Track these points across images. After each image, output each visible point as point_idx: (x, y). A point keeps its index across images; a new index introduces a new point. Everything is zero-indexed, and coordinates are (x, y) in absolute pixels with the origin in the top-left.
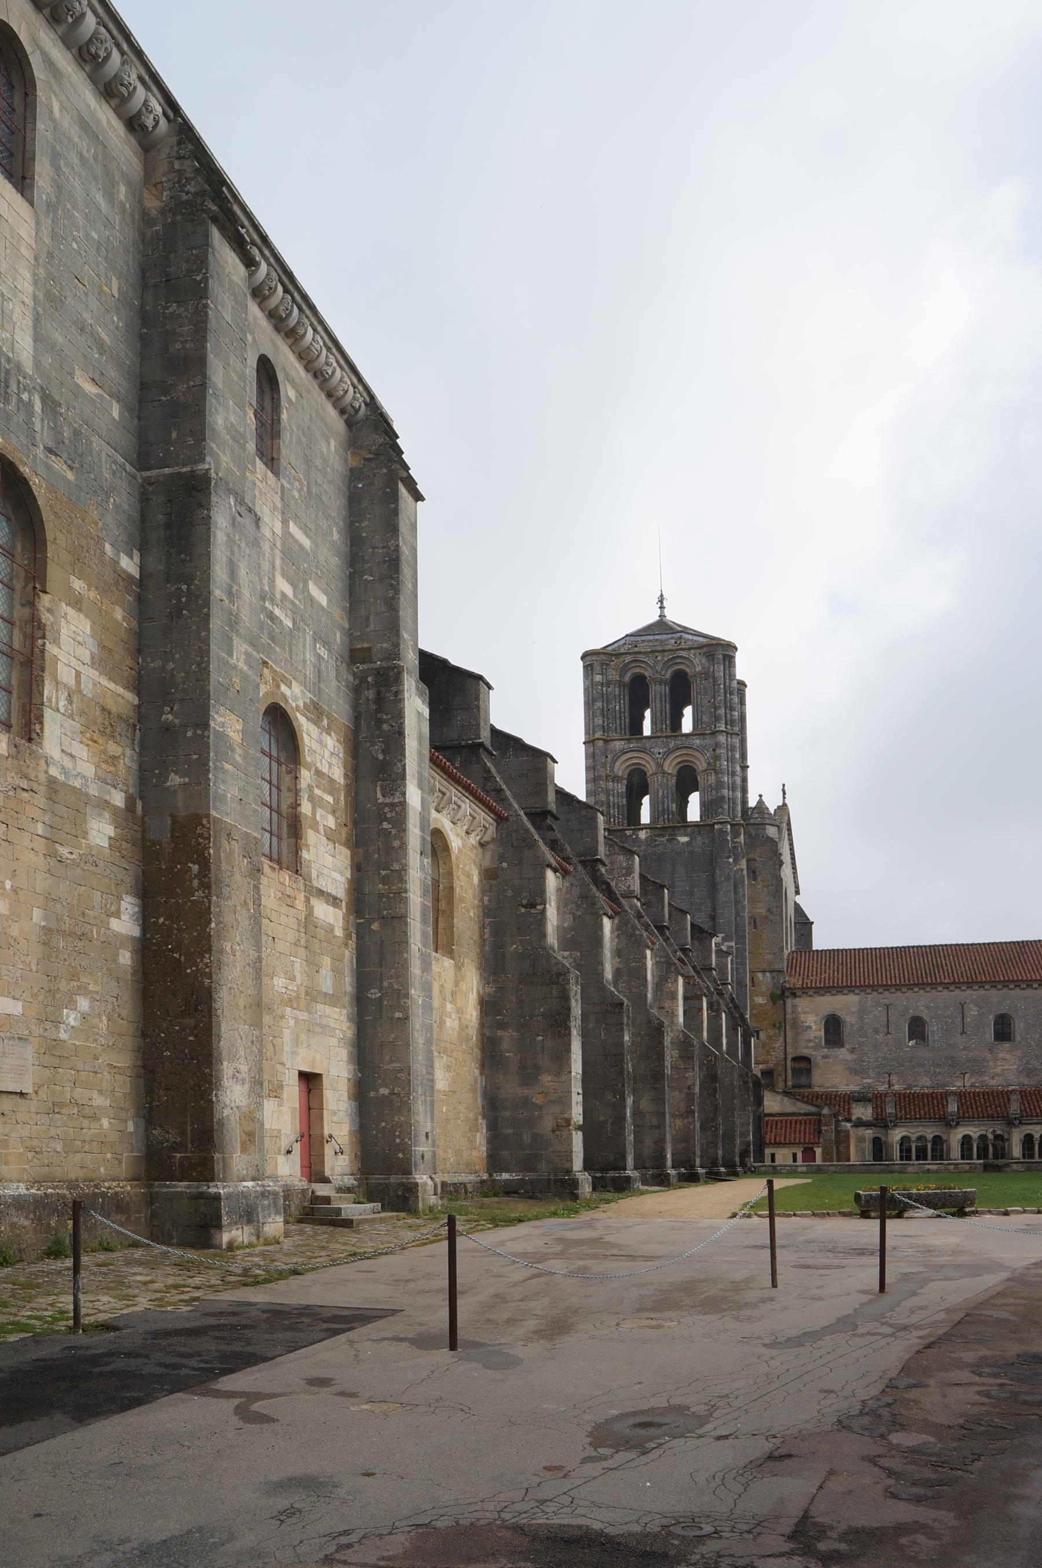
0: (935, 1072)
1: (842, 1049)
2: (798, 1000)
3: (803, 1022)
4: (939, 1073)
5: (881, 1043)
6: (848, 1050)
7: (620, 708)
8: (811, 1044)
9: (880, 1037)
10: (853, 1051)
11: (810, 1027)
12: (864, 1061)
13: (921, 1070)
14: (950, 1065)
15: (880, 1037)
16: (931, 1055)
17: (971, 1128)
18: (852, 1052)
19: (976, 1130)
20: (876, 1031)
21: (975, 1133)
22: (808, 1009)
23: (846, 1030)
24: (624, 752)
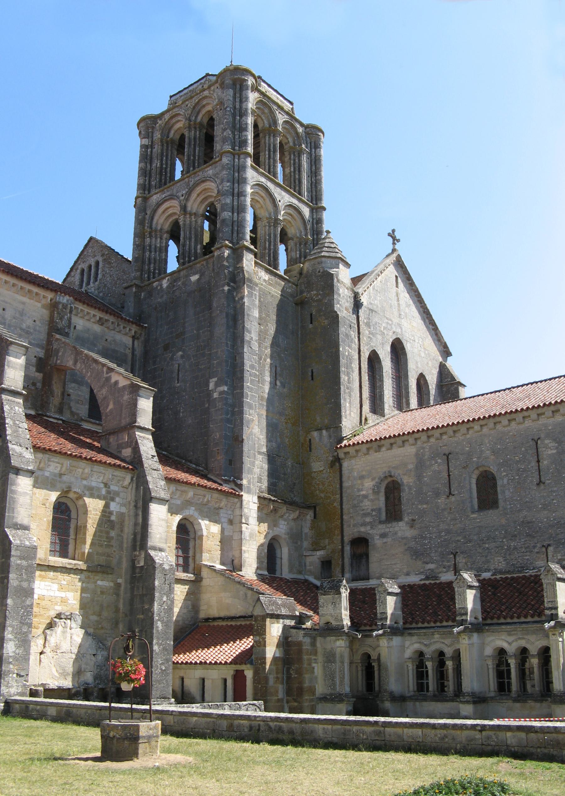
0: (509, 547)
1: (401, 524)
2: (353, 461)
3: (359, 490)
4: (515, 548)
5: (444, 510)
6: (407, 523)
7: (162, 164)
8: (368, 519)
9: (442, 501)
10: (412, 524)
11: (365, 497)
12: (425, 538)
13: (493, 545)
14: (528, 535)
15: (442, 501)
16: (503, 521)
17: (504, 636)
18: (412, 527)
19: (510, 639)
20: (437, 494)
21: (510, 644)
22: (364, 473)
23: (405, 495)
24: (159, 205)
